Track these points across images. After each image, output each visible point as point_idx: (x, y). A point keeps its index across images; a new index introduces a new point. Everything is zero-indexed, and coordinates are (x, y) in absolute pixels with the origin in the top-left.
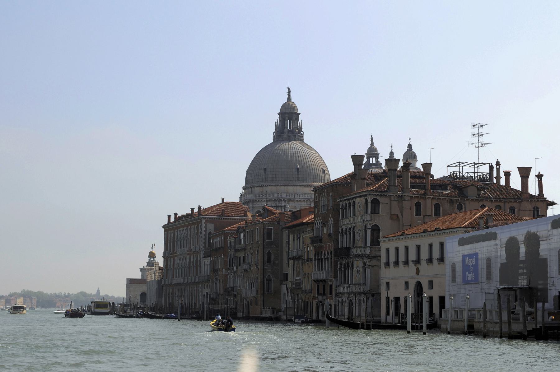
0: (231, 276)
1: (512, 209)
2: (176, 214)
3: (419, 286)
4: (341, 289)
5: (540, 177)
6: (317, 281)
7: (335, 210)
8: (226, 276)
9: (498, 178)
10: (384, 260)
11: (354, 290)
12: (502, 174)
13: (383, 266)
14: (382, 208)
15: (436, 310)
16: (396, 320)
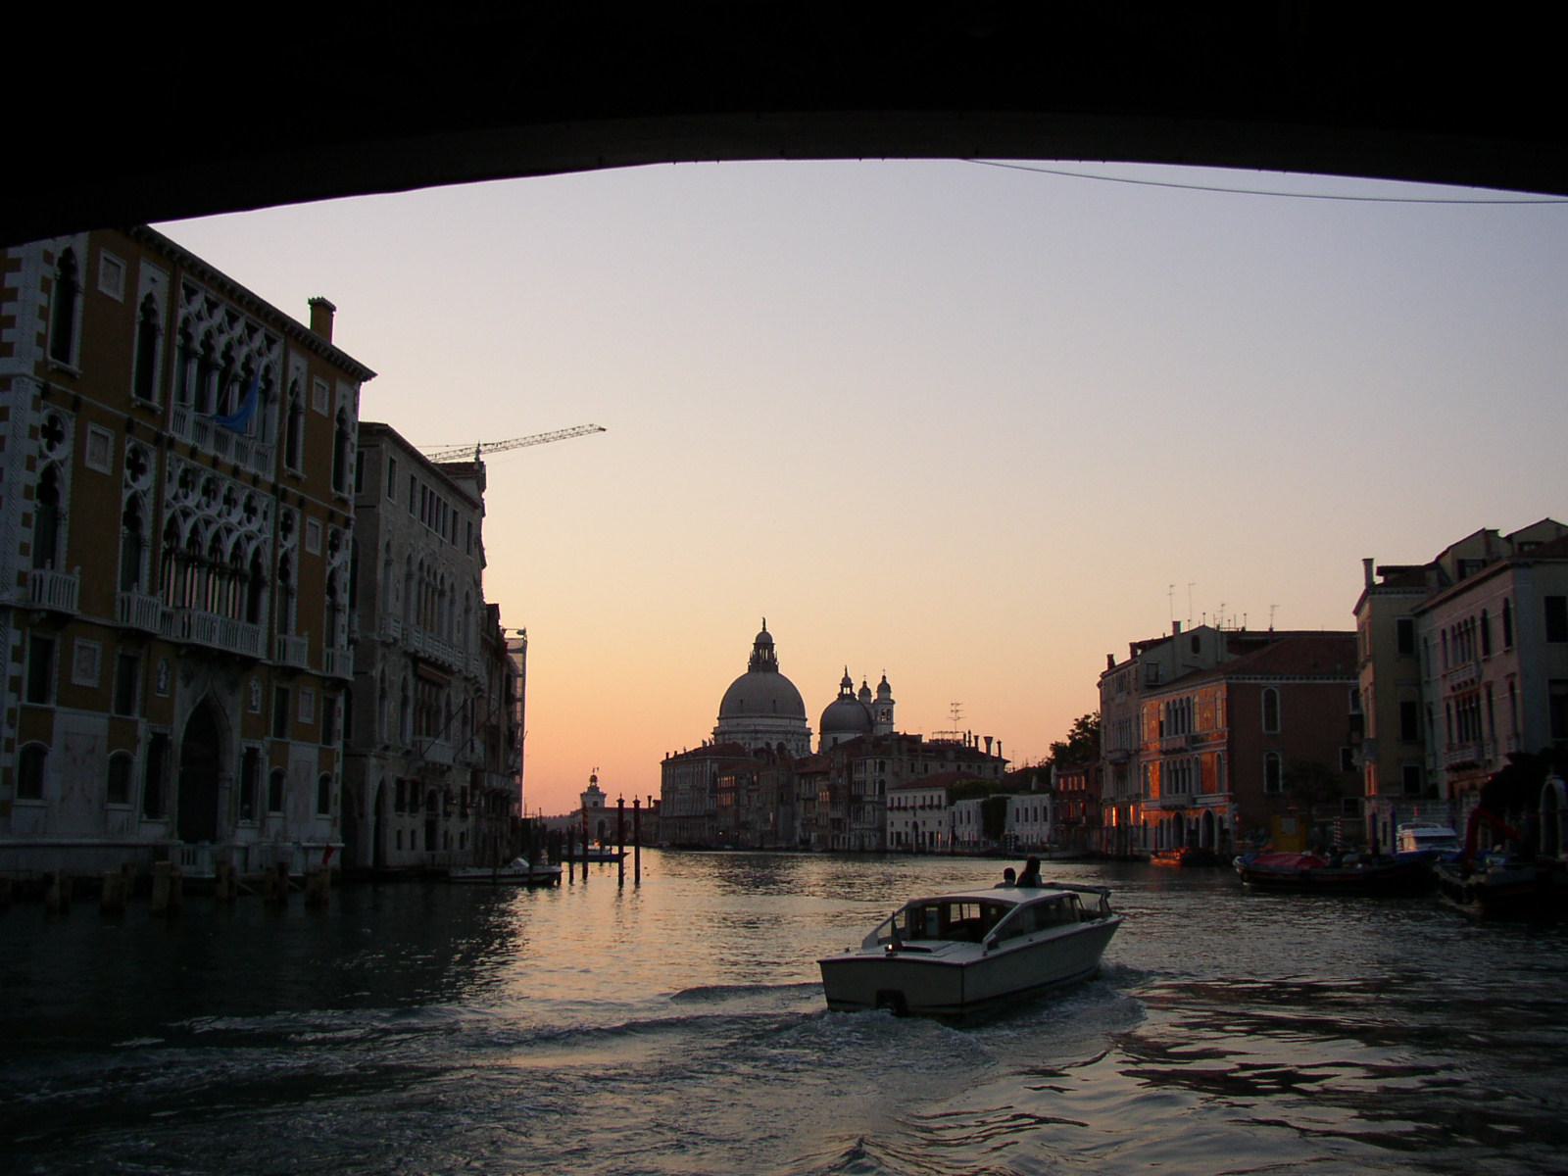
0: (743, 811)
1: (979, 767)
2: (676, 752)
3: (915, 825)
4: (854, 826)
5: (999, 743)
6: (833, 820)
7: (849, 767)
8: (737, 811)
9: (970, 742)
10: (889, 805)
11: (865, 827)
12: (973, 739)
13: (889, 812)
14: (886, 767)
15: (927, 841)
16: (900, 848)
